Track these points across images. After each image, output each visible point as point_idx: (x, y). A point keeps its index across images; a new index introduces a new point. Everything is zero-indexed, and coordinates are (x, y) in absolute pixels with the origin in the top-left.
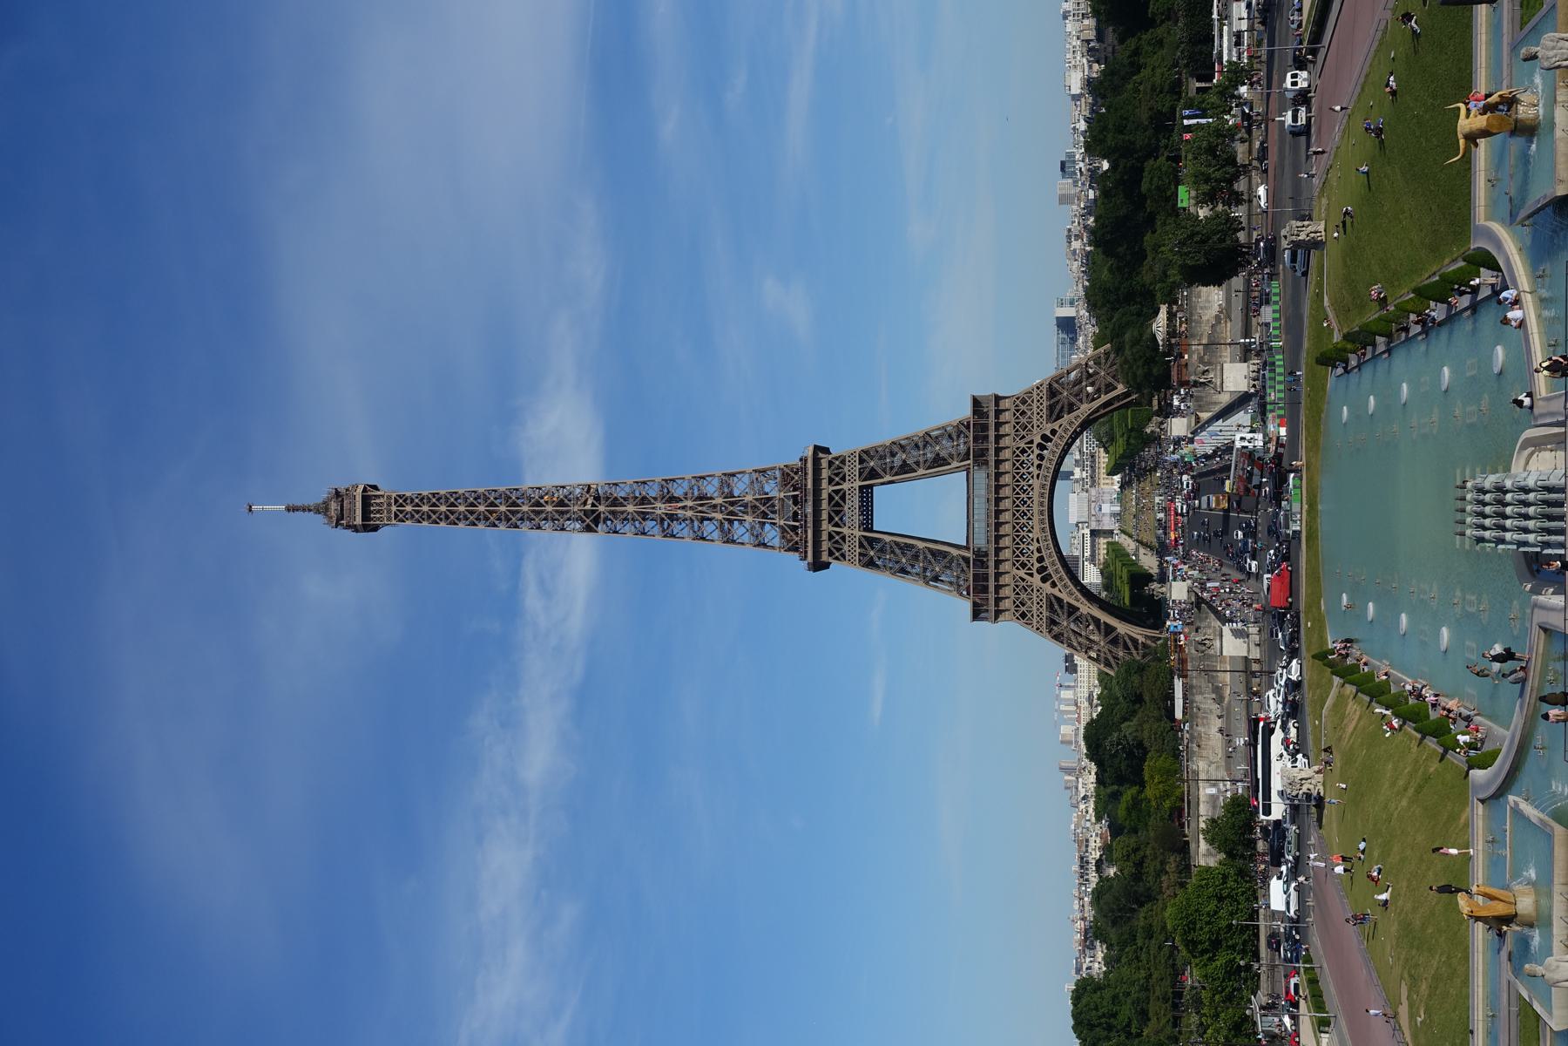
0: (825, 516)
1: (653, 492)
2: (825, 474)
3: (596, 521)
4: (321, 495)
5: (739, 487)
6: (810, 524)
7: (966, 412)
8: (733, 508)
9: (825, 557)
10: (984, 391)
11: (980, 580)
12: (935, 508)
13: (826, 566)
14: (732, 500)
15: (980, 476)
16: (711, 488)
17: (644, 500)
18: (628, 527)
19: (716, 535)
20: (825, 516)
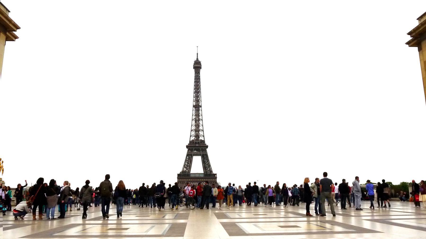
0: (196, 148)
1: (200, 117)
2: (203, 148)
3: (195, 108)
4: (199, 59)
5: (201, 133)
6: (194, 145)
7: (214, 173)
8: (197, 130)
9: (189, 148)
10: (218, 176)
11: (184, 176)
12: (197, 167)
13: (187, 148)
14: (199, 131)
15: (202, 176)
16: (201, 128)
17: (199, 116)
18: (194, 113)
19: (192, 129)
20: (196, 148)
